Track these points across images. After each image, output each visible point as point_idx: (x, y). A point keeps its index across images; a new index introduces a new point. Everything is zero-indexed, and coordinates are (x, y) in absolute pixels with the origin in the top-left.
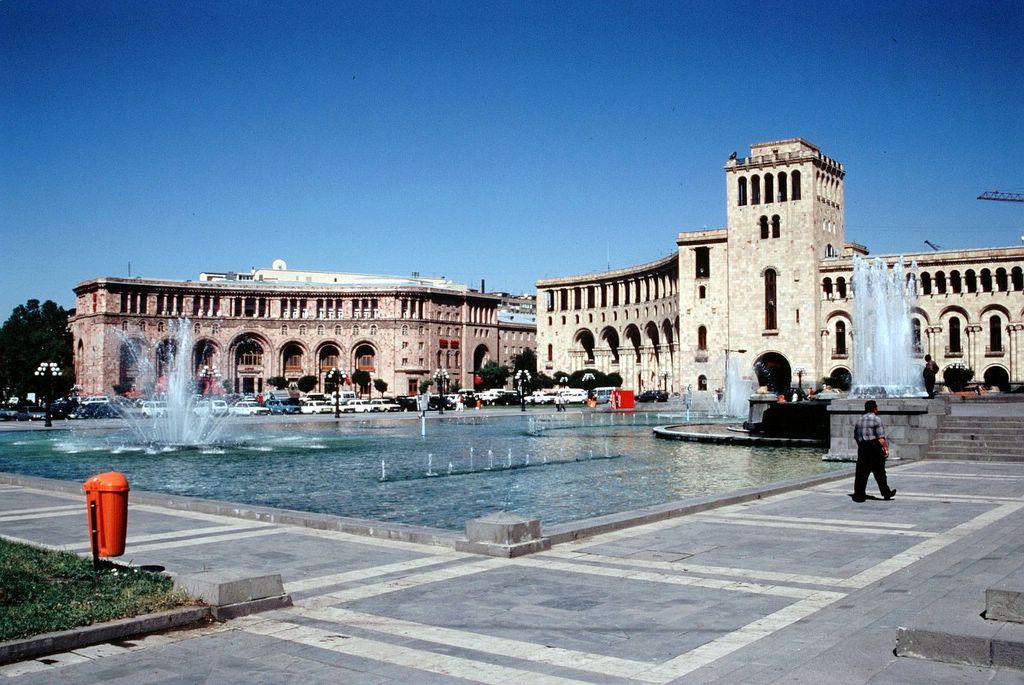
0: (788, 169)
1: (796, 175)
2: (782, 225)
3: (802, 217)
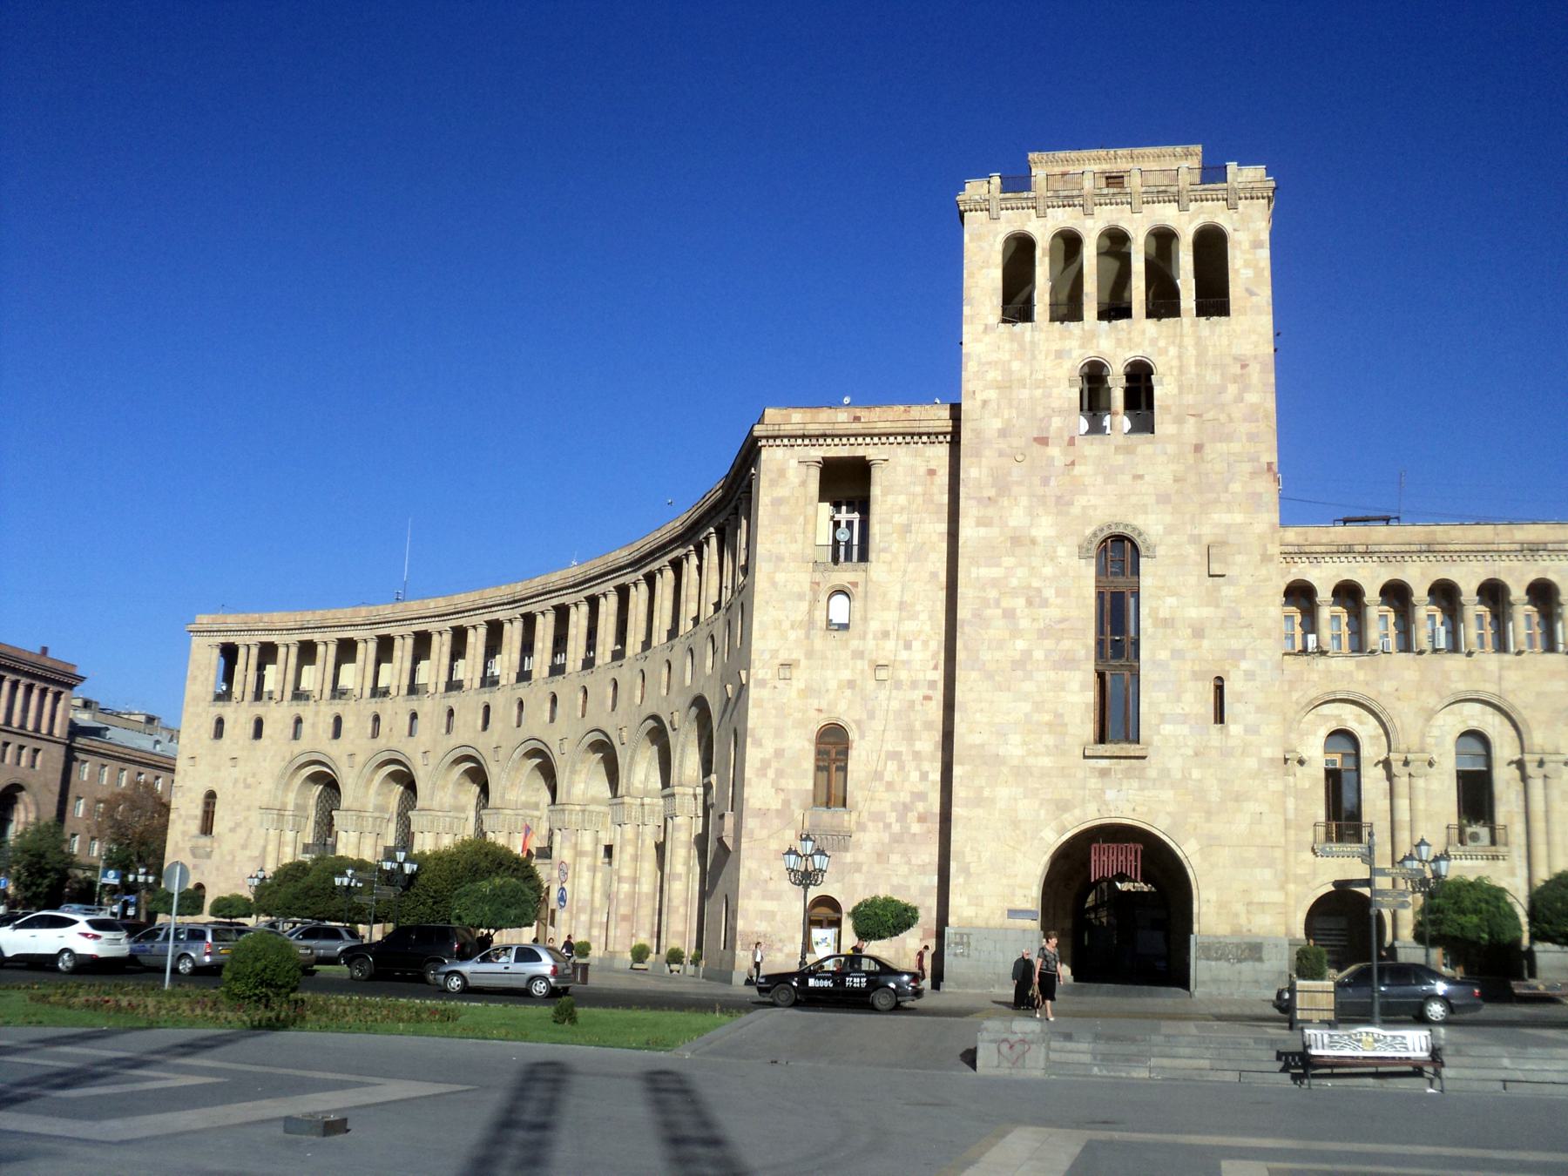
0: (1185, 216)
1: (1211, 245)
3: (1238, 370)
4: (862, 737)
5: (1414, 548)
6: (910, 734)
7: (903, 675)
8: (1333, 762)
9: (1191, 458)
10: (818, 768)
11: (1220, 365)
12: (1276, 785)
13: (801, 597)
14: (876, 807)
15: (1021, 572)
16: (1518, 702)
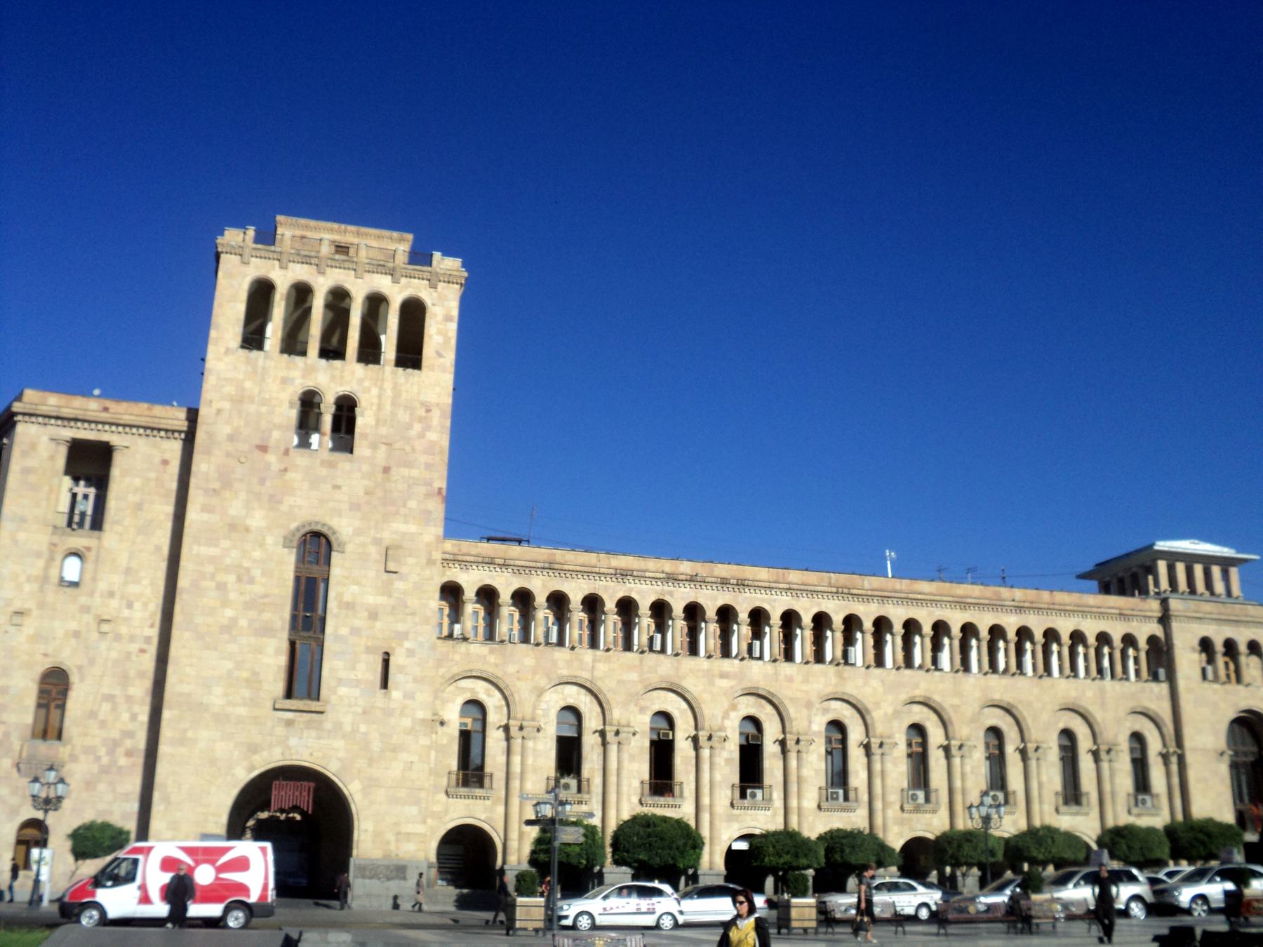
1: (414, 313)
2: (363, 421)
3: (422, 412)
4: (82, 680)
5: (539, 565)
6: (125, 680)
7: (124, 630)
8: (466, 725)
9: (380, 476)
10: (39, 706)
11: (411, 407)
12: (424, 741)
13: (38, 555)
14: (89, 741)
15: (234, 554)
16: (605, 687)
